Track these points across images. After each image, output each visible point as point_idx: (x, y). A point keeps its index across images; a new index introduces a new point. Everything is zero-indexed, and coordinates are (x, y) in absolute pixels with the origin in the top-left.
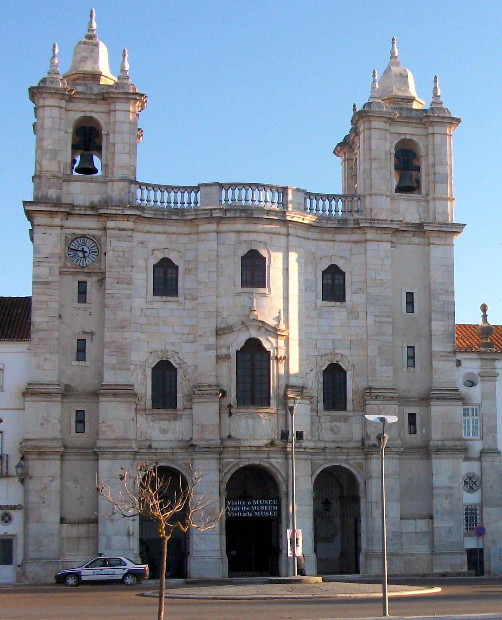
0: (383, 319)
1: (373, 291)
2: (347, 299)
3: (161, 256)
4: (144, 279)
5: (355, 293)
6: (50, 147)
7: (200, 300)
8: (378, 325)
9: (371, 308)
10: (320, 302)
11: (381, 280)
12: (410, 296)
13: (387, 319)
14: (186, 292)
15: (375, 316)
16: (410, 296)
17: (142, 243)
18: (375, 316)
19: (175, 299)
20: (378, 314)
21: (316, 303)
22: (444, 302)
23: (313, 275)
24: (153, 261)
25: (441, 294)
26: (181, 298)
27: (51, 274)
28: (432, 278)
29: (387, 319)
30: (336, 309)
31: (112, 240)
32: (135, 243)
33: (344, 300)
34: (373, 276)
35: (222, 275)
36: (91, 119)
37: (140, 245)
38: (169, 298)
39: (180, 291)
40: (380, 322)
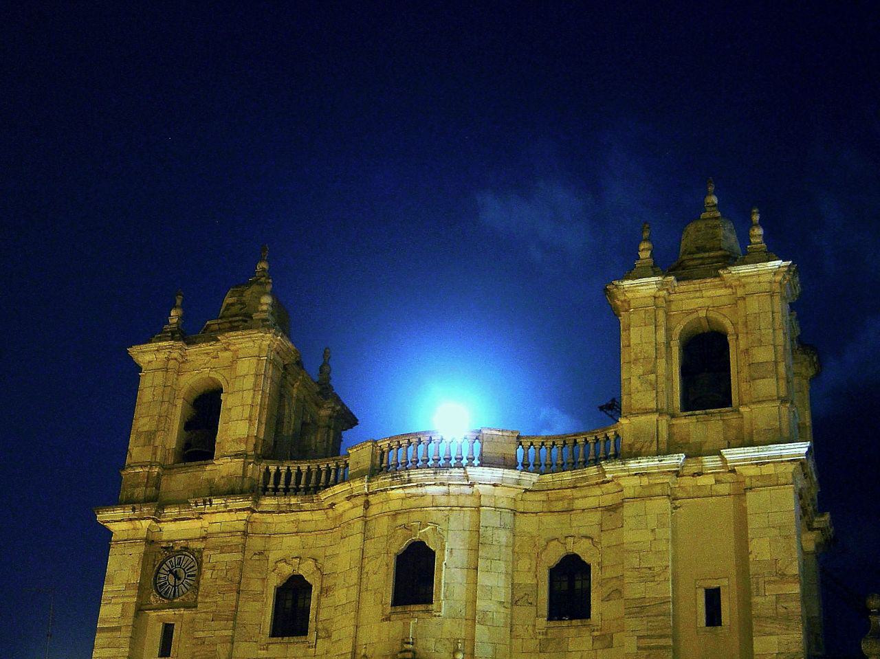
0: (654, 643)
1: (635, 590)
2: (594, 612)
3: (287, 570)
4: (261, 612)
5: (608, 598)
6: (146, 429)
7: (335, 637)
8: (646, 653)
9: (632, 623)
10: (542, 622)
11: (650, 568)
12: (713, 597)
13: (662, 642)
14: (320, 627)
15: (639, 637)
16: (713, 597)
17: (261, 553)
18: (639, 637)
19: (303, 638)
20: (645, 633)
21: (534, 626)
22: (778, 596)
23: (531, 574)
24: (275, 581)
25: (770, 582)
26: (312, 636)
27: (123, 616)
28: (751, 553)
29: (662, 642)
30: (573, 631)
31: (212, 552)
32: (248, 555)
33: (588, 616)
34: (635, 562)
35: (367, 590)
36: (213, 379)
37: (256, 557)
38: (295, 639)
39: (312, 625)
40: (650, 648)
